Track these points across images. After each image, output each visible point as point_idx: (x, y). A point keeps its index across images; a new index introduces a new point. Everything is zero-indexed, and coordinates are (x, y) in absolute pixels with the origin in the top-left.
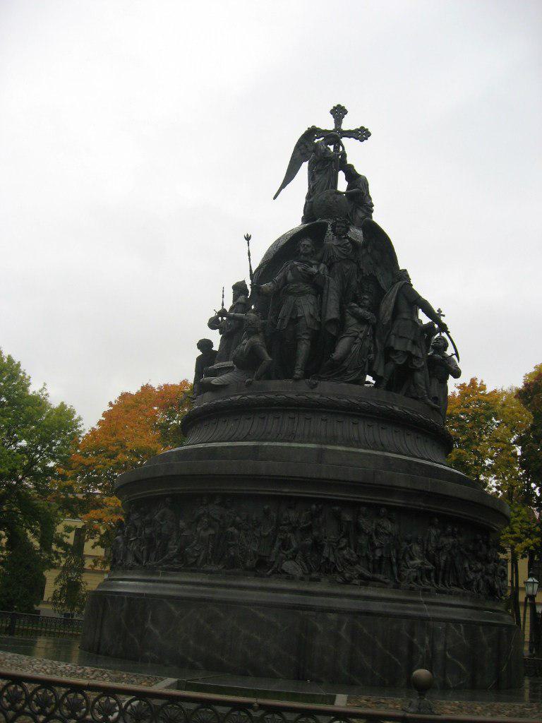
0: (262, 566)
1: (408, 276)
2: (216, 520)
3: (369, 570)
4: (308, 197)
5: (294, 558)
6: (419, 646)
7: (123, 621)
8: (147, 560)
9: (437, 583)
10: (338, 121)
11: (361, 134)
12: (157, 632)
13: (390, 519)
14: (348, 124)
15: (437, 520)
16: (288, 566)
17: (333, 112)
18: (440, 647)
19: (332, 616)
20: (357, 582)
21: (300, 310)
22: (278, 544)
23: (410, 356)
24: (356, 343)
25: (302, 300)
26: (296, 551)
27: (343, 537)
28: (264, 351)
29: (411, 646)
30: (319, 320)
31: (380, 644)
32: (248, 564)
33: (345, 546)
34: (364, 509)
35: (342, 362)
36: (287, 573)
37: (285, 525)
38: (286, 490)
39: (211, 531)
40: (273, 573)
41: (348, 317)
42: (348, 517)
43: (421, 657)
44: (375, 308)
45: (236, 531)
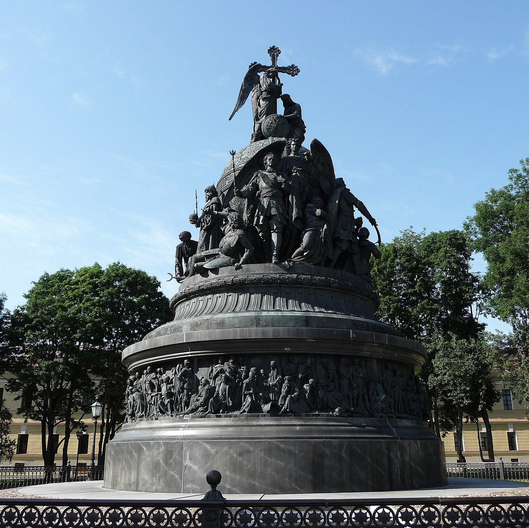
6: (394, 459)
10: (274, 60)
11: (292, 70)
12: (196, 467)
18: (407, 459)
31: (369, 460)
34: (343, 360)
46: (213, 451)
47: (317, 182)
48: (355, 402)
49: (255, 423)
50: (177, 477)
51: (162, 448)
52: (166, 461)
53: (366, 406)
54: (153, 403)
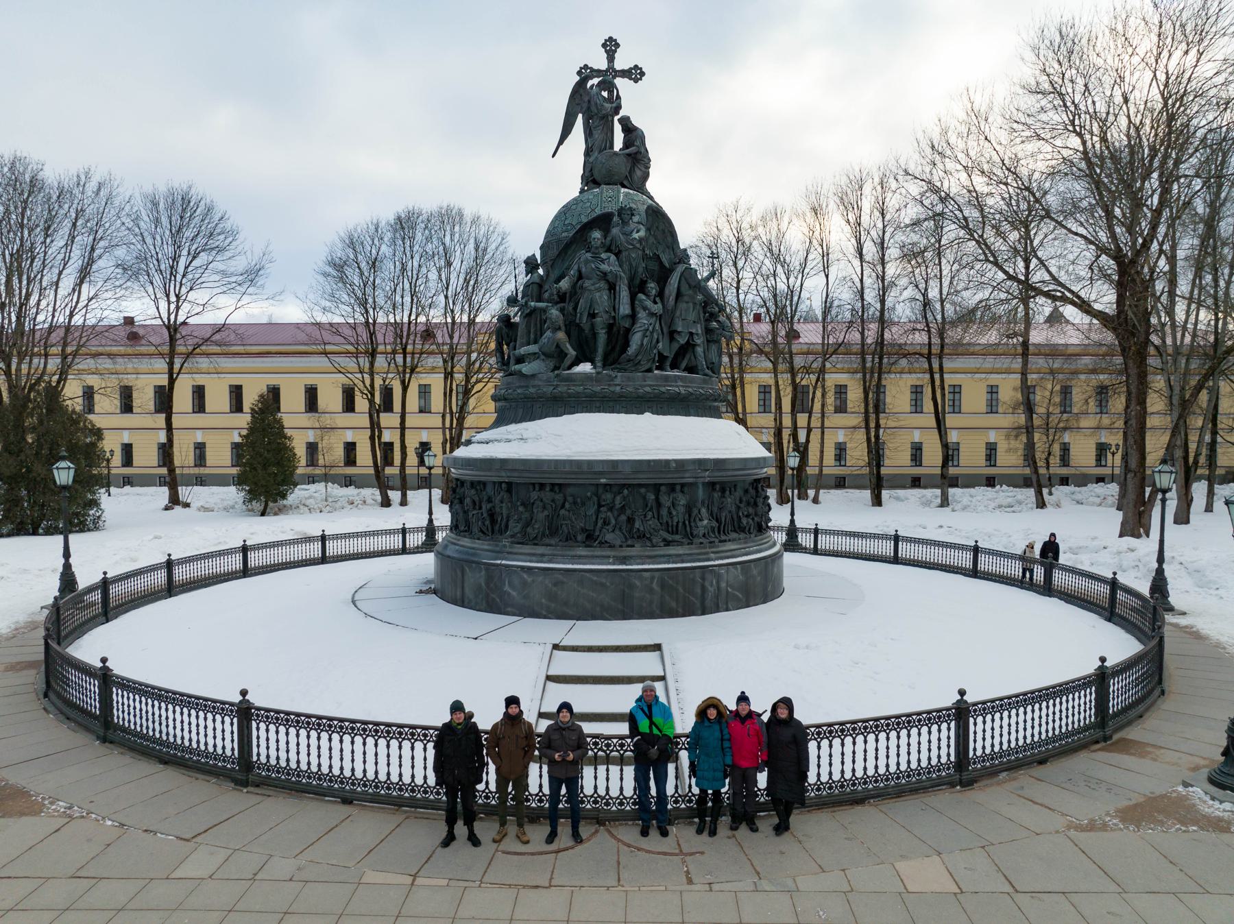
0: (590, 538)
5: (613, 531)
8: (493, 532)
9: (719, 532)
10: (611, 59)
11: (635, 74)
12: (514, 593)
14: (619, 65)
16: (609, 537)
17: (604, 45)
18: (723, 585)
19: (647, 574)
20: (662, 544)
21: (597, 307)
23: (691, 334)
28: (568, 346)
29: (704, 588)
30: (613, 314)
31: (681, 590)
32: (580, 538)
35: (637, 356)
39: (546, 513)
44: (661, 294)
46: (530, 580)
49: (568, 553)
52: (487, 584)
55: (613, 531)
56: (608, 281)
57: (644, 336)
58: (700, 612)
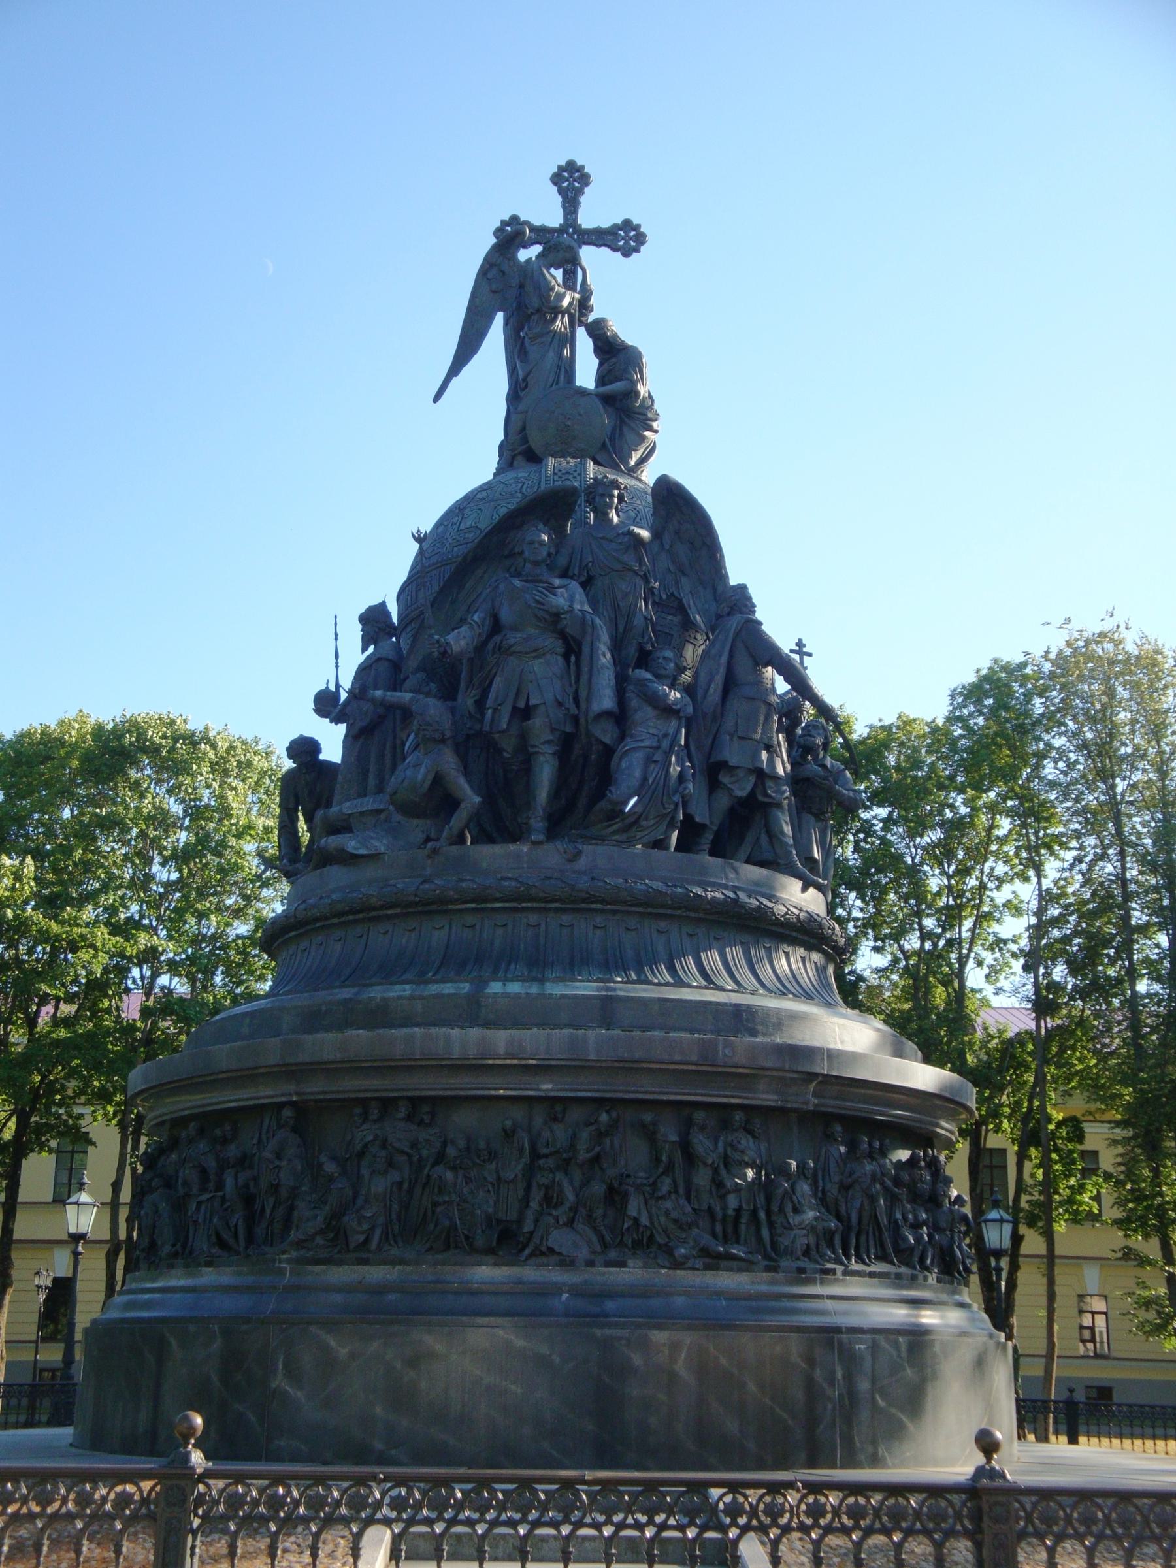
1: (750, 599)
2: (403, 1152)
3: (714, 1236)
4: (514, 397)
5: (570, 1223)
6: (825, 1385)
7: (215, 1379)
8: (250, 1239)
10: (571, 203)
12: (300, 1395)
13: (750, 1132)
14: (590, 216)
15: (839, 1128)
16: (560, 1239)
17: (556, 179)
20: (699, 1263)
22: (537, 1196)
24: (655, 762)
25: (537, 667)
26: (574, 1209)
27: (663, 1174)
28: (462, 781)
29: (810, 1385)
30: (573, 710)
31: (752, 1387)
32: (480, 1241)
33: (670, 1192)
34: (699, 1116)
36: (560, 1254)
37: (546, 1156)
38: (547, 1087)
39: (394, 1176)
40: (531, 1255)
41: (634, 703)
42: (669, 1133)
43: (830, 1406)
45: (449, 1175)
46: (343, 1352)
47: (672, 594)
48: (730, 1230)
50: (253, 1419)
51: (217, 1344)
53: (760, 1239)
54: (200, 1220)
55: (570, 1223)
56: (563, 635)
57: (649, 760)
58: (803, 1456)
